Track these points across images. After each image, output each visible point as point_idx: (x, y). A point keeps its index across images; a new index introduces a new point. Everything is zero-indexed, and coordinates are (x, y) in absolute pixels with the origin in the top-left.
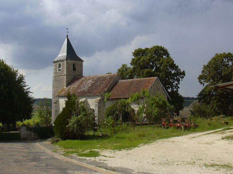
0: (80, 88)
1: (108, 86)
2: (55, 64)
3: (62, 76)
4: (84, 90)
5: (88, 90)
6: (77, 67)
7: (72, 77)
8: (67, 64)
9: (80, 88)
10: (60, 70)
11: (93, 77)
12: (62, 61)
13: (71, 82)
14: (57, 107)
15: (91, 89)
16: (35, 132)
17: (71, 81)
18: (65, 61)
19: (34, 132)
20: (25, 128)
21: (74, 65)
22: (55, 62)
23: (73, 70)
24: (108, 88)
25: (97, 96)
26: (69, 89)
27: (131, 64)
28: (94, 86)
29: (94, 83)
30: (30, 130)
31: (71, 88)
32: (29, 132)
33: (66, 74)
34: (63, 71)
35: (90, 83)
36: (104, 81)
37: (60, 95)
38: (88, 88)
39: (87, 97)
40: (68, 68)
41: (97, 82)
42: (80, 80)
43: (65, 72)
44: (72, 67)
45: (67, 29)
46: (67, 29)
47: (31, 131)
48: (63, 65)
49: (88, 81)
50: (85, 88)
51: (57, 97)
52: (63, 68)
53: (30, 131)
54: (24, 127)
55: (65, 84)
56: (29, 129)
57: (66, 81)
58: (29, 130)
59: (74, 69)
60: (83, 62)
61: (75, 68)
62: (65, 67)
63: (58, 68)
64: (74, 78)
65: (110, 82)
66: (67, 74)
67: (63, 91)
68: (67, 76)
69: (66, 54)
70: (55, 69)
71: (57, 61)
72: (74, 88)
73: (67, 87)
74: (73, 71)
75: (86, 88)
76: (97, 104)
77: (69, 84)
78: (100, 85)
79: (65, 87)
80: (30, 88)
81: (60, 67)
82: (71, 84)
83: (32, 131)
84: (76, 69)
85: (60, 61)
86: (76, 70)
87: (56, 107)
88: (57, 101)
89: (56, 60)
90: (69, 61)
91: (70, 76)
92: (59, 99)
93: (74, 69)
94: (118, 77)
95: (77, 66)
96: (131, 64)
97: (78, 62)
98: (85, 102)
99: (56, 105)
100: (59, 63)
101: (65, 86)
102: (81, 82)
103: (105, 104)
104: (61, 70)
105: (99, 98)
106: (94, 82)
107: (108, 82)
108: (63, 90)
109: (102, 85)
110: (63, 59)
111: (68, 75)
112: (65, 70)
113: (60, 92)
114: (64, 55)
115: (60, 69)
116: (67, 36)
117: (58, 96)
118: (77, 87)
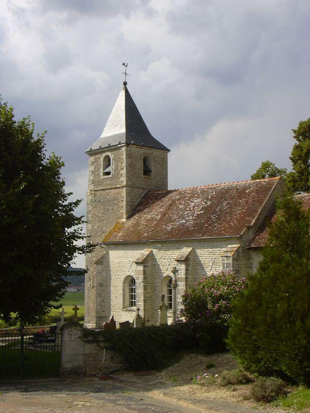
0: (170, 220)
1: (257, 212)
2: (92, 159)
3: (113, 191)
4: (183, 225)
5: (195, 225)
6: (153, 167)
7: (141, 191)
8: (129, 156)
9: (170, 220)
10: (108, 173)
11: (203, 191)
12: (111, 148)
13: (138, 205)
14: (104, 274)
15: (207, 222)
16: (112, 348)
17: (140, 204)
18: (124, 149)
19: (106, 348)
20: (76, 332)
21: (145, 160)
22: (92, 153)
23: (144, 174)
24: (258, 219)
25: (229, 240)
26: (137, 225)
27: (294, 160)
28: (213, 214)
29: (211, 206)
30: (94, 341)
31: (143, 221)
32: (89, 348)
33: (125, 183)
34: (118, 175)
35: (198, 206)
36: (241, 199)
37: (112, 240)
38: (195, 220)
39: (196, 244)
40: (130, 167)
41: (220, 203)
42: (166, 199)
43: (124, 179)
44: (140, 165)
45: (124, 64)
46: (124, 64)
47: (99, 346)
48: (118, 160)
49: (192, 202)
50: (187, 221)
51: (104, 246)
52: (116, 168)
53: (94, 345)
54: (73, 328)
55: (124, 211)
56: (90, 338)
57: (127, 202)
58: (88, 342)
59: (147, 171)
60: (169, 154)
61: (148, 168)
62: (124, 164)
63: (102, 170)
64: (146, 195)
65: (260, 202)
66: (130, 183)
67: (119, 229)
68: (128, 188)
69: (124, 130)
70: (93, 172)
71: (101, 150)
72: (152, 219)
73: (129, 218)
74: (143, 176)
75: (189, 221)
76: (230, 261)
77: (134, 210)
78: (231, 211)
79: (124, 220)
80: (72, 193)
81: (109, 165)
82: (140, 211)
83: (102, 344)
84: (151, 171)
85: (108, 151)
86: (152, 173)
87: (101, 274)
88: (102, 257)
89: (95, 147)
90: (134, 149)
91: (136, 190)
92: (110, 252)
93: (147, 171)
94: (280, 187)
95: (152, 164)
96: (291, 158)
97: (157, 153)
98: (191, 257)
99: (100, 267)
100: (104, 155)
101: (125, 216)
102: (171, 205)
103: (252, 264)
104: (113, 172)
105: (236, 246)
106: (209, 203)
107: (254, 201)
108: (119, 227)
109: (238, 211)
110: (117, 143)
111: (130, 186)
112: (124, 172)
113: (111, 233)
114: (117, 132)
115: (107, 170)
116: (125, 84)
117: (105, 244)
118: (159, 217)
